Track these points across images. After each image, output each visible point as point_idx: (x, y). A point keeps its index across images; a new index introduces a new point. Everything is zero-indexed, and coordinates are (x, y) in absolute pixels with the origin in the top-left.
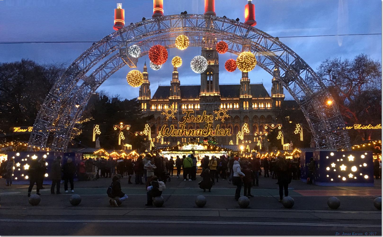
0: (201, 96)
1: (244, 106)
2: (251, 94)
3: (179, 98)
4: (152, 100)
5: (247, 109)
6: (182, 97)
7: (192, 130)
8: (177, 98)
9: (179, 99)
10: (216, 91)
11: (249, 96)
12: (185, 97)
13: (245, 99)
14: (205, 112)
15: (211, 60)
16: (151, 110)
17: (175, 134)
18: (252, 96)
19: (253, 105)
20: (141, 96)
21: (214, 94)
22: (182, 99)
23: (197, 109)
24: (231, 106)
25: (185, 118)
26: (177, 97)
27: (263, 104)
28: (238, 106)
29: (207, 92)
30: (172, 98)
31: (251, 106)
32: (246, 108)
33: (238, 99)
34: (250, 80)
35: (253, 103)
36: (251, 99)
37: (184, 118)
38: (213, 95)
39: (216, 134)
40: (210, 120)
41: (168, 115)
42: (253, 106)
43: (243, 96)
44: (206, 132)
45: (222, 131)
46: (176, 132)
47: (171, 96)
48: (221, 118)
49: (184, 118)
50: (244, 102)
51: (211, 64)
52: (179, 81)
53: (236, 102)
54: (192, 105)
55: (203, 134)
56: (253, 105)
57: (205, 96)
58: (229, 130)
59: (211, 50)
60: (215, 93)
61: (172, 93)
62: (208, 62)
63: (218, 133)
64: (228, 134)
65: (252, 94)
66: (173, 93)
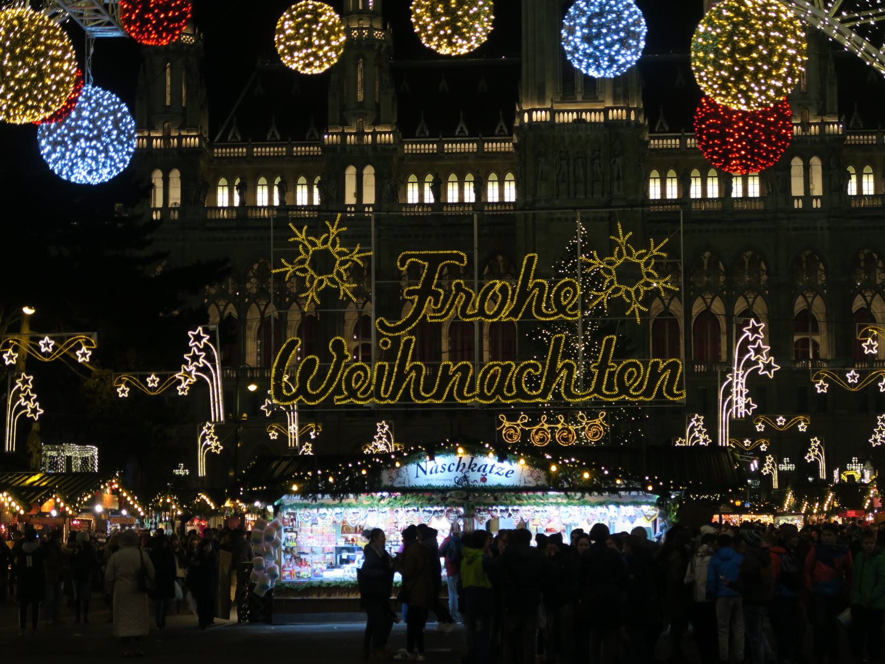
1: (797, 188)
2: (836, 108)
3: (388, 138)
4: (218, 152)
5: (817, 204)
6: (406, 131)
8: (374, 138)
11: (823, 125)
14: (531, 260)
16: (211, 215)
17: (353, 393)
19: (854, 179)
20: (151, 128)
21: (606, 111)
23: (502, 203)
24: (713, 190)
25: (416, 298)
26: (374, 134)
28: (754, 189)
29: (563, 100)
30: (344, 135)
32: (808, 197)
35: (851, 169)
36: (838, 139)
37: (410, 293)
38: (599, 118)
39: (598, 390)
40: (561, 309)
41: (312, 279)
42: (852, 189)
44: (542, 374)
45: (631, 373)
46: (359, 377)
47: (335, 124)
48: (628, 294)
49: (410, 293)
54: (470, 177)
55: (521, 394)
56: (854, 179)
58: (674, 367)
60: (609, 104)
63: (610, 387)
64: (670, 392)
65: (844, 113)
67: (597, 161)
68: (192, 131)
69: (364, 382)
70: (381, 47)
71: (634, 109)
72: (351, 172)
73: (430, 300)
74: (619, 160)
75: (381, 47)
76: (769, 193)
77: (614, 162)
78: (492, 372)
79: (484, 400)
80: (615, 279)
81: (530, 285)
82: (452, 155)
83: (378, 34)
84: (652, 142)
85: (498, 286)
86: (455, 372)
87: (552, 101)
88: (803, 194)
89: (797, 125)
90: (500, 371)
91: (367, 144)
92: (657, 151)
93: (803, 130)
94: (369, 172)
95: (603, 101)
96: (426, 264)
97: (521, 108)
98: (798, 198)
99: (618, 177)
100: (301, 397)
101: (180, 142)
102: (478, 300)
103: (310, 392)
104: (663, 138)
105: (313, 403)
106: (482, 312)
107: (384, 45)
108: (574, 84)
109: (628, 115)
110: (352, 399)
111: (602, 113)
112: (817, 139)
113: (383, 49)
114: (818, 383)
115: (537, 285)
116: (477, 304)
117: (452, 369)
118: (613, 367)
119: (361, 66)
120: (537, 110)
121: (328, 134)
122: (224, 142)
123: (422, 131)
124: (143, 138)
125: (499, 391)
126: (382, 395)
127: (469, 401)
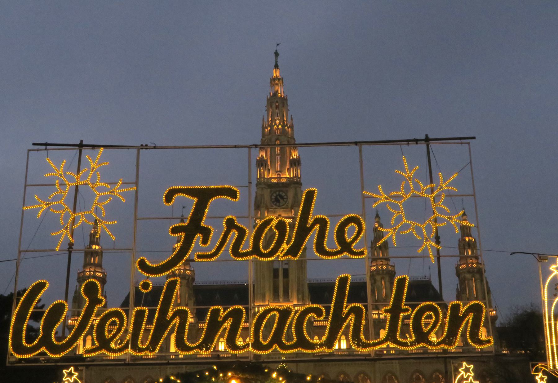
7: (222, 314)
10: (300, 296)
15: (285, 211)
34: (394, 267)
43: (379, 314)
52: (193, 271)
59: (283, 183)
69: (119, 330)
70: (189, 279)
73: (199, 238)
75: (189, 279)
78: (268, 317)
79: (259, 350)
80: (403, 214)
81: (310, 221)
84: (315, 323)
85: (274, 223)
86: (225, 319)
87: (269, 301)
90: (278, 315)
95: (292, 302)
96: (195, 199)
97: (254, 305)
100: (43, 349)
102: (252, 238)
103: (56, 343)
105: (57, 356)
106: (256, 250)
108: (279, 294)
110: (104, 351)
113: (190, 279)
114: (538, 375)
115: (317, 221)
116: (251, 242)
117: (222, 314)
118: (407, 310)
124: (75, 320)
125: (277, 339)
126: (140, 345)
127: (241, 352)
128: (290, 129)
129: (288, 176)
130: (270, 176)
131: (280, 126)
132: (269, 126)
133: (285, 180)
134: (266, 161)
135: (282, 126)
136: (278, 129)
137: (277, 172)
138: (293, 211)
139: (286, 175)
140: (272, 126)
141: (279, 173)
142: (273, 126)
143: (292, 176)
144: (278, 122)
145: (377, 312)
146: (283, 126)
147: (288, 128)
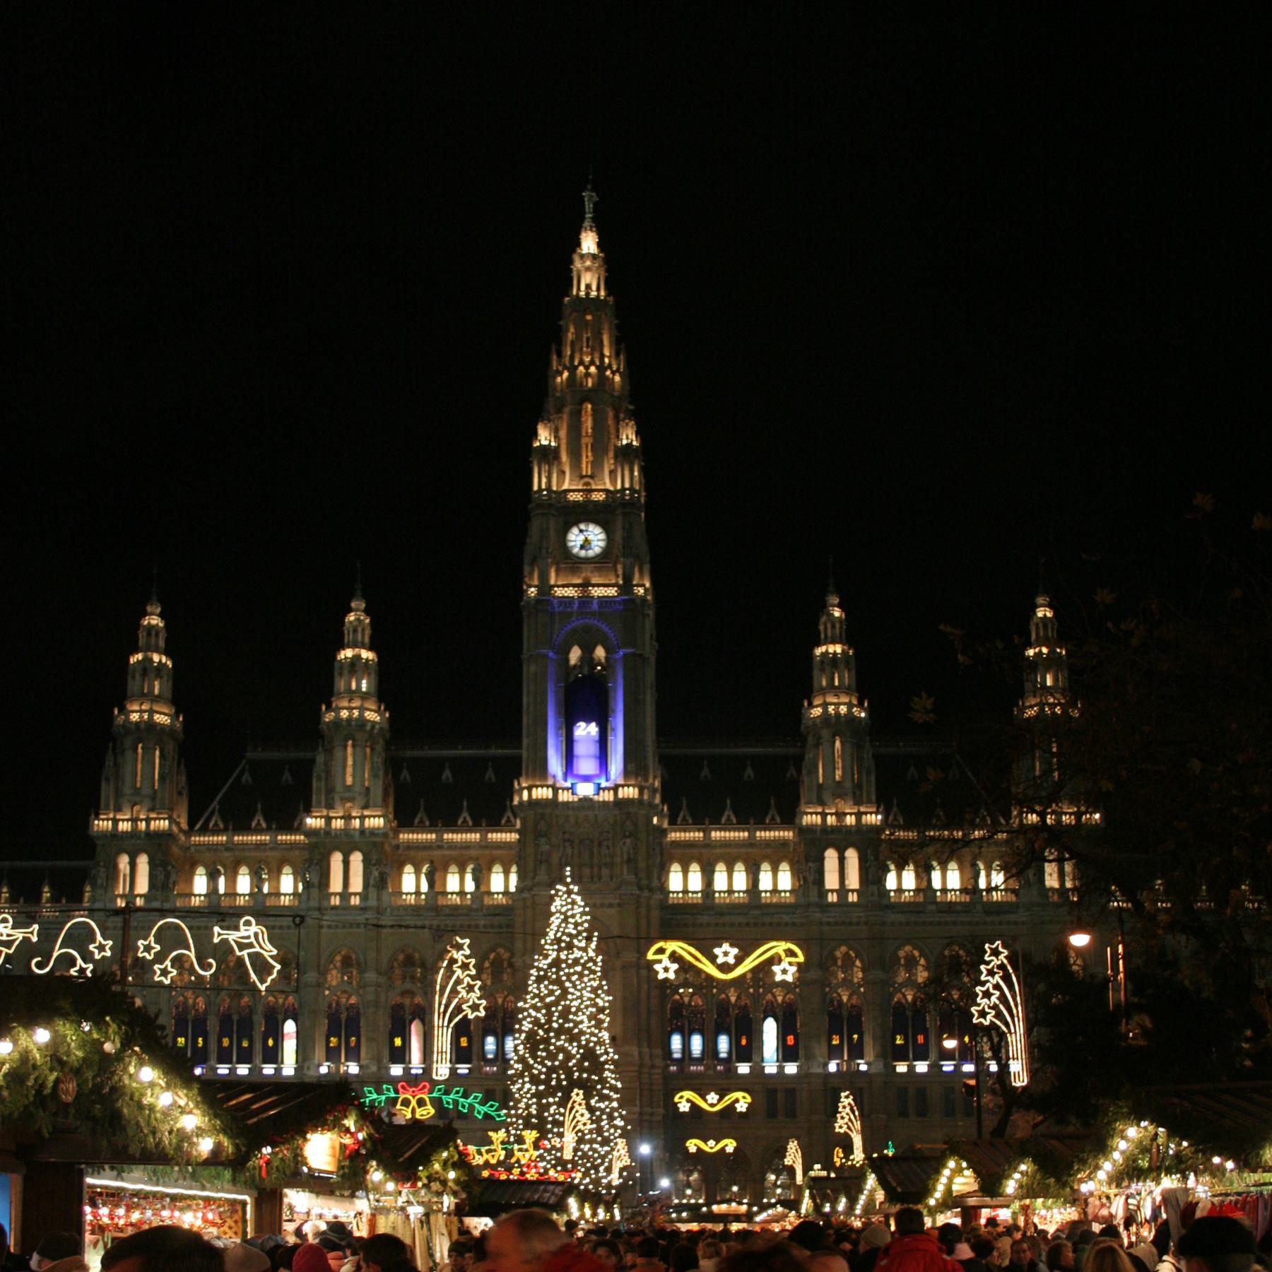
0: (521, 803)
1: (831, 881)
4: (196, 839)
5: (853, 898)
8: (362, 823)
9: (373, 832)
12: (421, 821)
13: (834, 829)
15: (599, 570)
18: (886, 816)
22: (396, 832)
26: (362, 818)
27: (961, 870)
30: (329, 819)
31: (881, 881)
32: (843, 891)
33: (788, 834)
42: (891, 882)
43: (824, 815)
50: (831, 856)
51: (597, 592)
53: (775, 854)
57: (554, 802)
61: (330, 791)
62: (579, 581)
65: (883, 802)
66: (339, 788)
67: (605, 843)
68: (161, 813)
71: (648, 788)
72: (336, 860)
74: (628, 841)
75: (373, 727)
76: (800, 886)
77: (624, 843)
82: (452, 845)
83: (371, 716)
88: (836, 886)
89: (831, 814)
91: (354, 829)
92: (676, 844)
93: (838, 821)
94: (357, 859)
98: (832, 891)
99: (629, 861)
101: (148, 825)
104: (685, 831)
107: (377, 726)
109: (641, 793)
111: (612, 792)
112: (854, 829)
113: (376, 731)
119: (350, 750)
120: (537, 787)
121: (312, 817)
122: (204, 830)
123: (421, 821)
124: (108, 820)
128: (617, 378)
129: (612, 489)
130: (566, 486)
131: (593, 369)
132: (565, 368)
133: (600, 497)
134: (557, 450)
135: (597, 368)
136: (588, 375)
137: (582, 477)
138: (620, 567)
139: (605, 484)
140: (573, 370)
141: (587, 480)
142: (576, 368)
143: (619, 487)
144: (587, 359)
145: (820, 810)
146: (601, 369)
147: (613, 373)
